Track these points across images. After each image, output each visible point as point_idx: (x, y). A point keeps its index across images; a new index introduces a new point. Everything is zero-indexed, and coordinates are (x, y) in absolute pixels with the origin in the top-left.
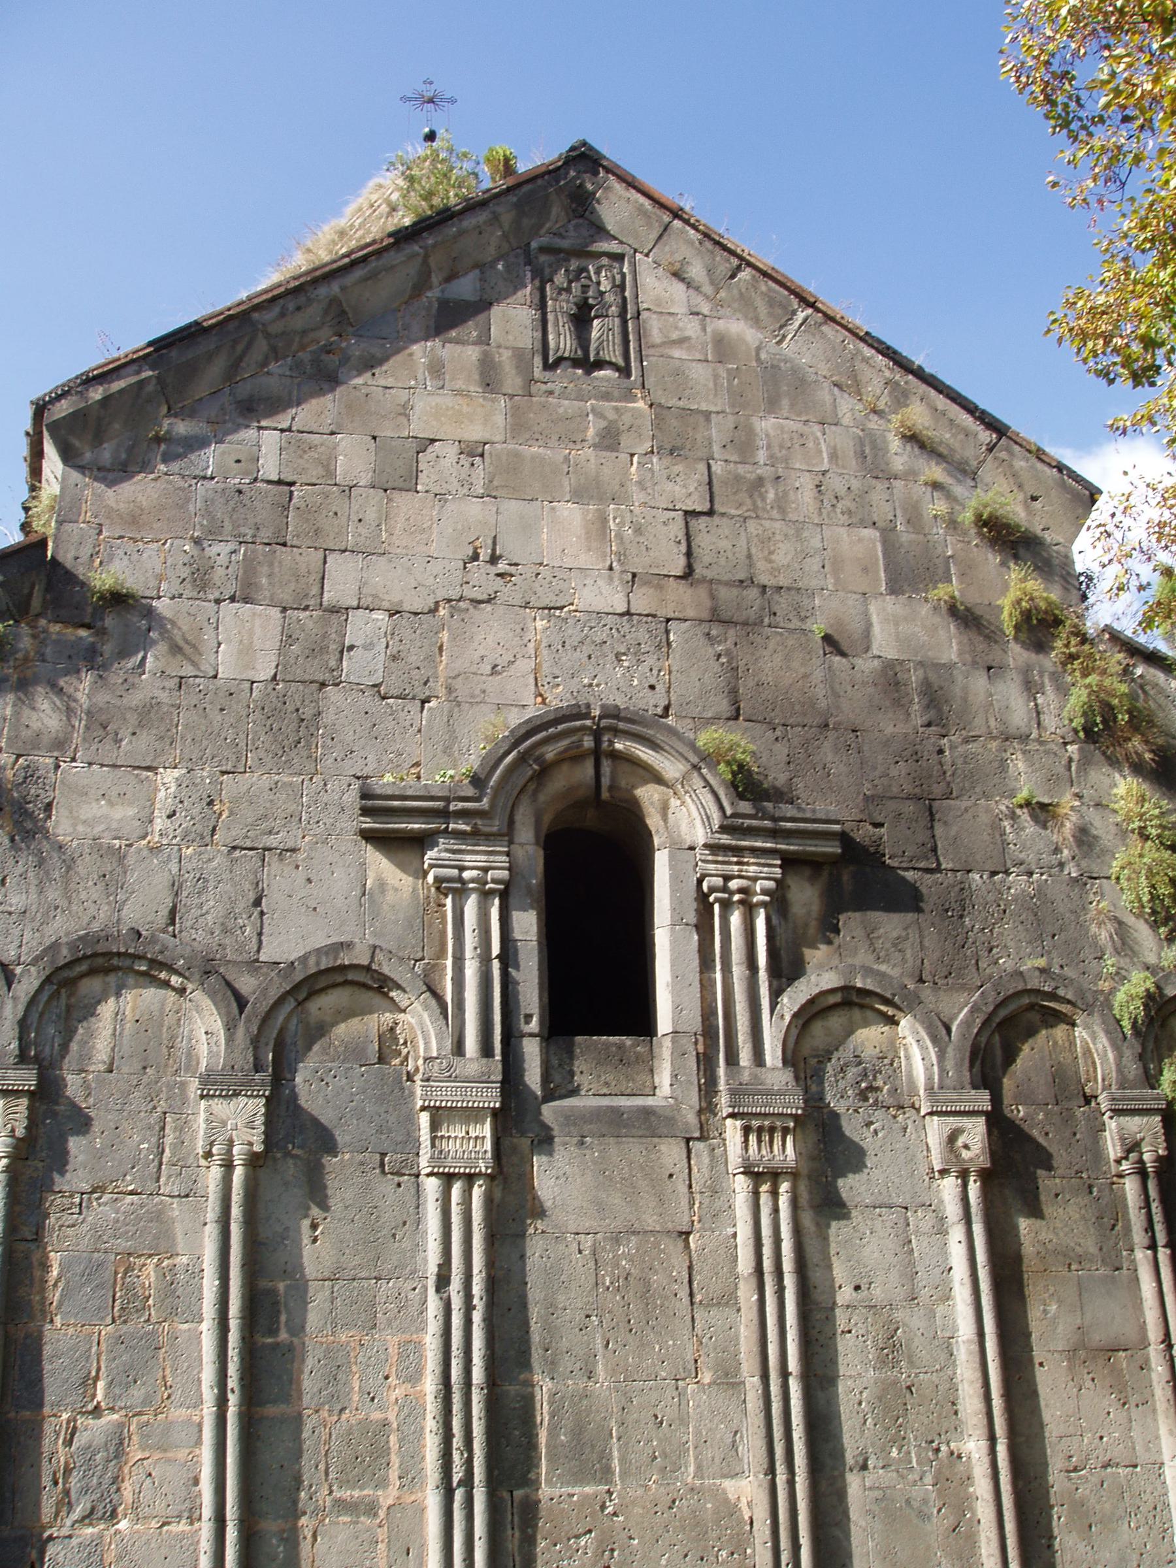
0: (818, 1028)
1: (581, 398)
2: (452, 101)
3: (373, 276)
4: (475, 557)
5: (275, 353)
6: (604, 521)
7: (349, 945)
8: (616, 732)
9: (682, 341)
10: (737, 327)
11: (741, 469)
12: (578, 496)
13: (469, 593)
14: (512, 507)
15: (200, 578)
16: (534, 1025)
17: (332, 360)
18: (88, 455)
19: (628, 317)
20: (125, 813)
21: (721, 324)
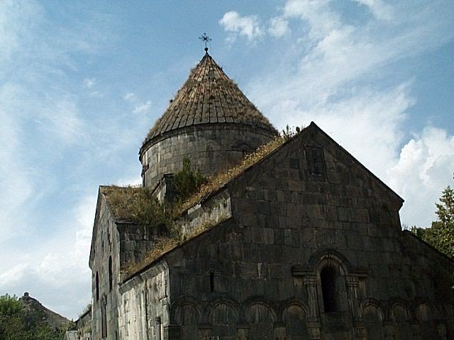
0: (365, 310)
1: (316, 181)
2: (211, 40)
3: (279, 155)
4: (304, 217)
5: (264, 172)
6: (323, 207)
7: (294, 297)
8: (331, 254)
9: (332, 168)
10: (341, 164)
11: (345, 197)
12: (319, 203)
13: (304, 225)
14: (308, 205)
15: (259, 223)
16: (323, 311)
17: (273, 172)
18: (234, 195)
19: (324, 162)
20: (254, 272)
21: (338, 164)
